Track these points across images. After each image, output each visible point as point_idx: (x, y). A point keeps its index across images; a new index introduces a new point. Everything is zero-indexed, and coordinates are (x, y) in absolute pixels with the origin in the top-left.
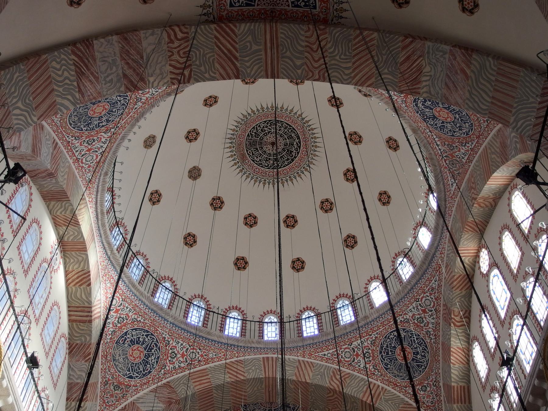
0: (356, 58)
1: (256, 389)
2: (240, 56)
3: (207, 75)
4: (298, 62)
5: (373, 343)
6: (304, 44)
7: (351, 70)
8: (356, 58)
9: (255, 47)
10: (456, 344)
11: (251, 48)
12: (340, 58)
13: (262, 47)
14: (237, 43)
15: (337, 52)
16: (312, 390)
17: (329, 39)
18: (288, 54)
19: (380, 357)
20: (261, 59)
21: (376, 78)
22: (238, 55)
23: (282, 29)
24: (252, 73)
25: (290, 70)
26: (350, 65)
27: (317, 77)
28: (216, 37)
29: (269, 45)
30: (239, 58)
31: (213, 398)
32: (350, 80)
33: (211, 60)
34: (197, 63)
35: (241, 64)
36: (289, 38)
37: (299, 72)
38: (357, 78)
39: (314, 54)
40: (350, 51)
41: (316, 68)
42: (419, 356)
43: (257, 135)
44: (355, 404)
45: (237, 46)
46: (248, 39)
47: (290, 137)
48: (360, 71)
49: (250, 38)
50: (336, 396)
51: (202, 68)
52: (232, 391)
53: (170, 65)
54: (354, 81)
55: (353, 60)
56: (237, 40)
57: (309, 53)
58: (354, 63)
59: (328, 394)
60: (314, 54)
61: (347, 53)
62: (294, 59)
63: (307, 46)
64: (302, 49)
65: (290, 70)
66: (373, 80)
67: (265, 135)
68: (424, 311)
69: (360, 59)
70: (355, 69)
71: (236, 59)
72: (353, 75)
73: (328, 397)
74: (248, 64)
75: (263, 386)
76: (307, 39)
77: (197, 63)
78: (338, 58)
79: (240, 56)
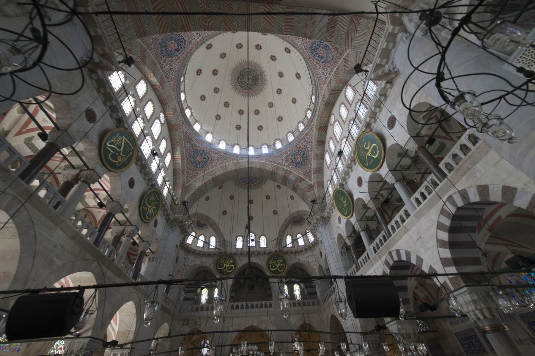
1: (258, 20)
5: (190, 42)
10: (153, 79)
16: (223, 24)
19: (185, 38)
31: (286, 22)
42: (164, 49)
43: (255, 84)
44: (193, 23)
47: (242, 82)
50: (207, 25)
52: (273, 22)
59: (212, 24)
67: (251, 83)
68: (171, 69)
73: (211, 20)
75: (253, 21)
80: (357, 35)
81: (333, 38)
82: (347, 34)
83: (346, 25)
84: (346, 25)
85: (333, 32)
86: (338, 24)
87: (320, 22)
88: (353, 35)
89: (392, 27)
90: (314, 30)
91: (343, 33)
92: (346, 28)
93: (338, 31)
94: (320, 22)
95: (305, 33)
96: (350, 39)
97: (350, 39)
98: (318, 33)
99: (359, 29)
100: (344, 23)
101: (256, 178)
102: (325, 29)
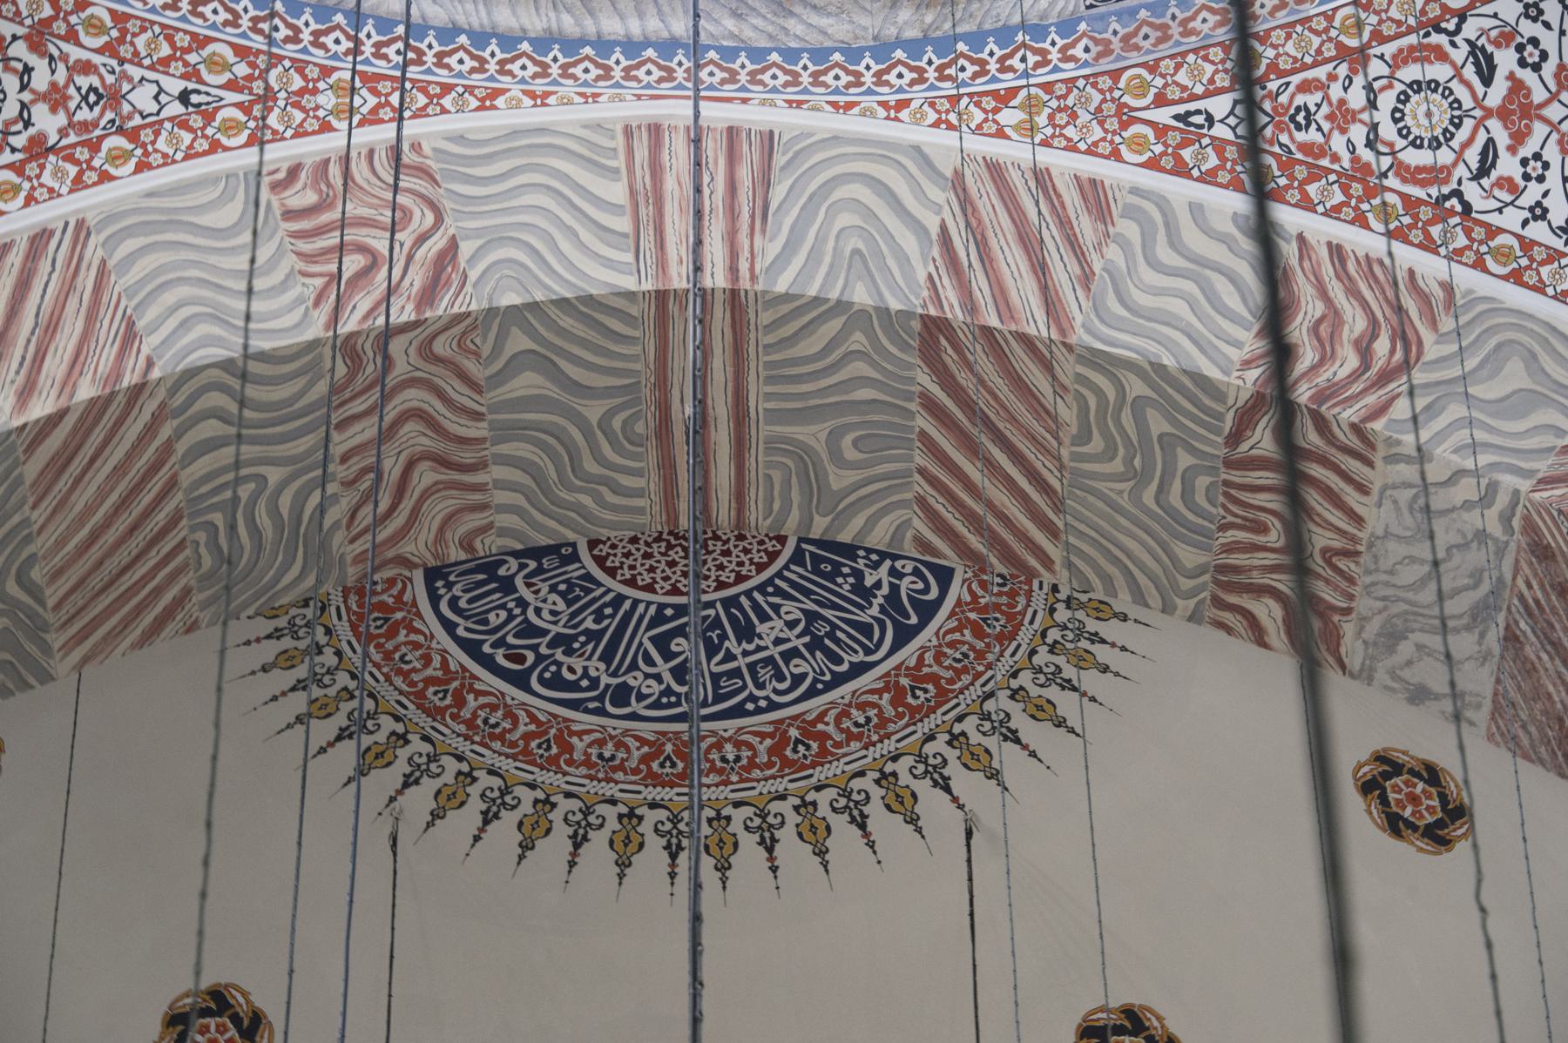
0: (161, 518)
2: (911, 415)
3: (1136, 388)
4: (527, 383)
6: (499, 472)
7: (181, 448)
8: (161, 518)
9: (813, 434)
11: (835, 436)
12: (263, 479)
13: (762, 431)
14: (922, 472)
15: (285, 502)
17: (339, 537)
18: (593, 411)
20: (770, 380)
21: (19, 481)
22: (923, 422)
23: (640, 511)
24: (836, 324)
25: (584, 343)
26: (187, 476)
27: (396, 346)
28: (1053, 532)
29: (721, 437)
30: (913, 406)
32: (179, 399)
33: (1097, 444)
34: (1184, 460)
35: (911, 380)
36: (590, 478)
37: (519, 342)
38: (133, 429)
39: (428, 442)
40: (202, 536)
41: (411, 382)
45: (920, 459)
46: (853, 477)
48: (120, 470)
49: (838, 479)
51: (1158, 425)
53: (1358, 520)
54: (151, 407)
55: (177, 498)
56: (921, 486)
57: (462, 441)
58: (172, 484)
60: (428, 442)
61: (218, 518)
62: (553, 391)
63: (481, 466)
64: (504, 449)
65: (584, 343)
66: (31, 470)
69: (134, 528)
70: (154, 468)
71: (930, 405)
72: (166, 432)
74: (860, 368)
76: (477, 497)
77: (1184, 460)
78: (274, 475)
79: (911, 415)
101: (830, 557)
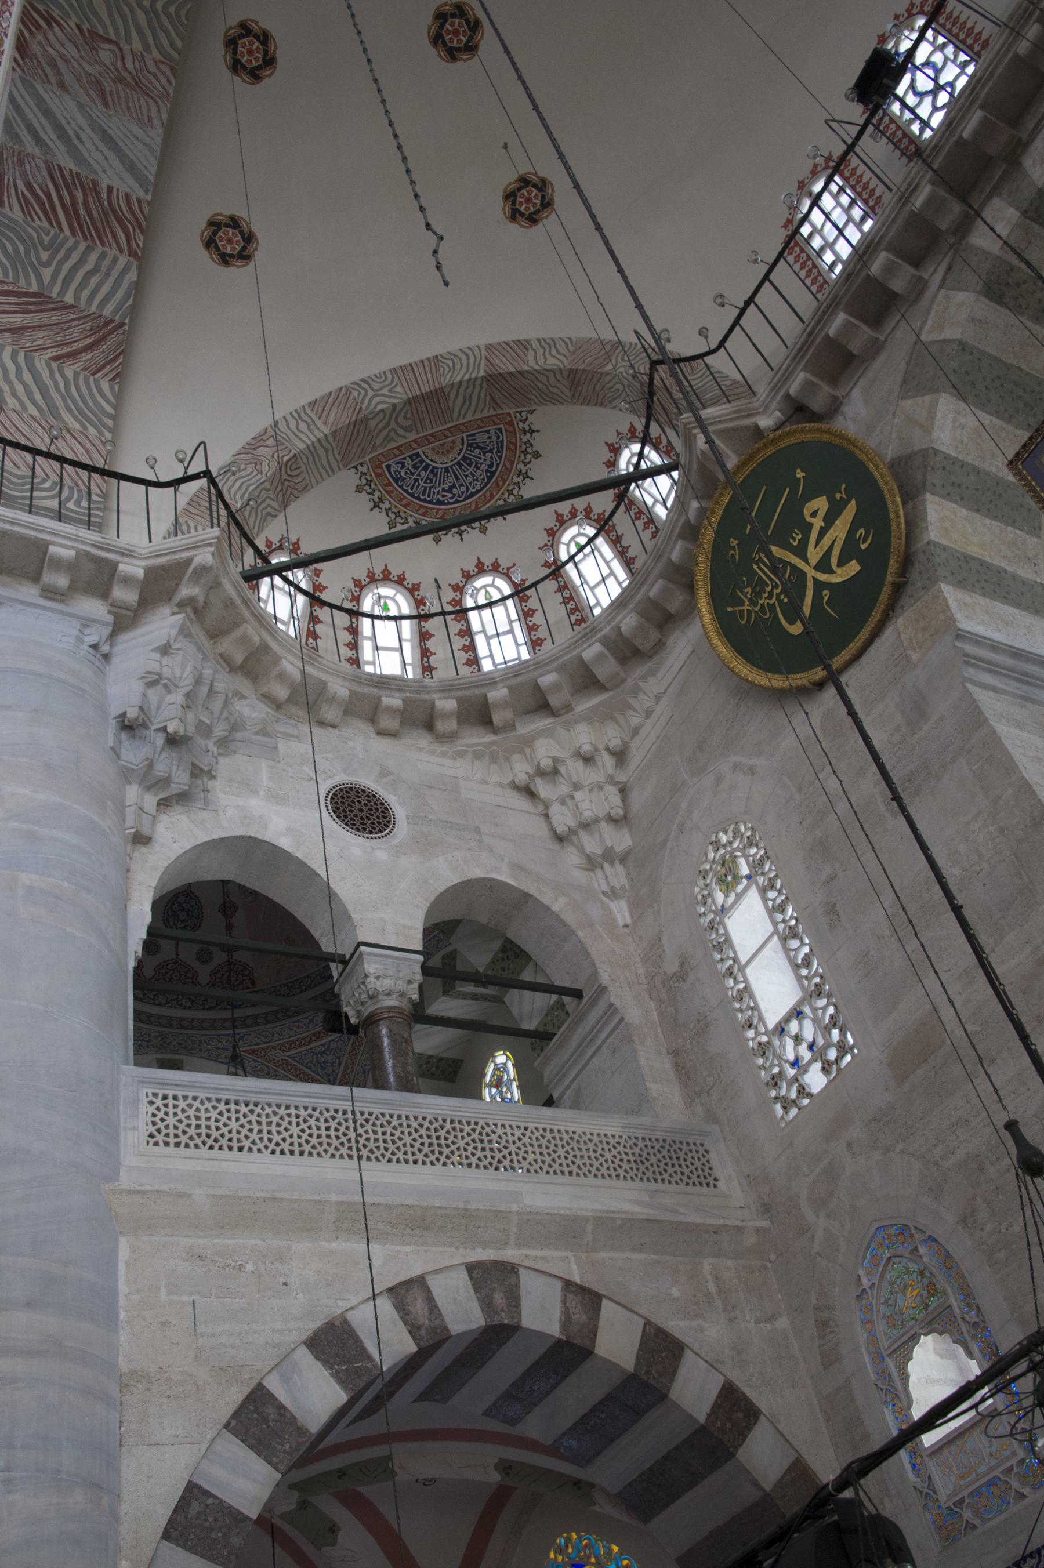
80: (40, 362)
81: (17, 214)
82: (41, 301)
83: (86, 293)
84: (86, 293)
85: (49, 215)
86: (88, 250)
87: (107, 138)
88: (40, 338)
89: (140, 573)
90: (62, 85)
91: (47, 273)
92: (69, 298)
93: (53, 247)
94: (107, 138)
95: (49, 20)
96: (16, 319)
97: (16, 319)
98: (47, 113)
99: (69, 373)
100: (94, 280)
102: (68, 164)
